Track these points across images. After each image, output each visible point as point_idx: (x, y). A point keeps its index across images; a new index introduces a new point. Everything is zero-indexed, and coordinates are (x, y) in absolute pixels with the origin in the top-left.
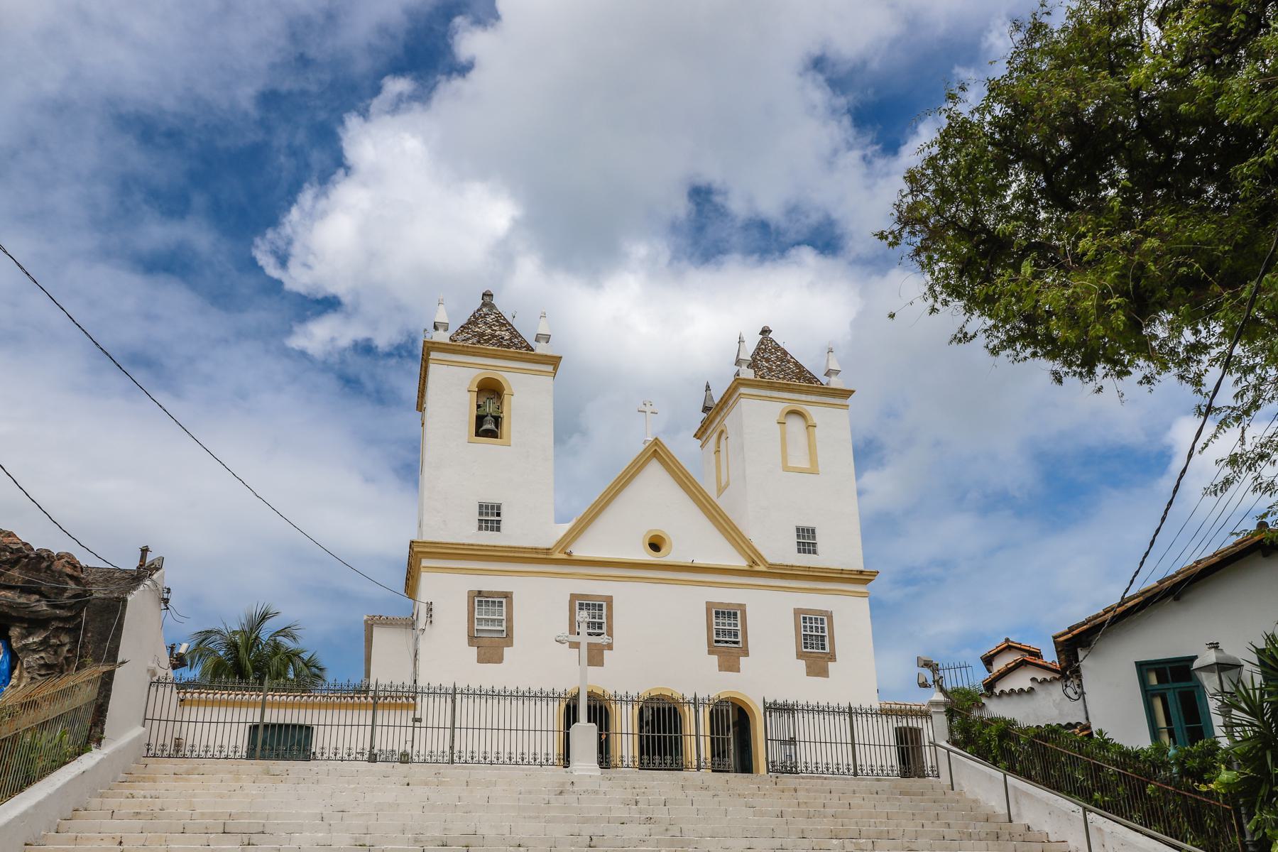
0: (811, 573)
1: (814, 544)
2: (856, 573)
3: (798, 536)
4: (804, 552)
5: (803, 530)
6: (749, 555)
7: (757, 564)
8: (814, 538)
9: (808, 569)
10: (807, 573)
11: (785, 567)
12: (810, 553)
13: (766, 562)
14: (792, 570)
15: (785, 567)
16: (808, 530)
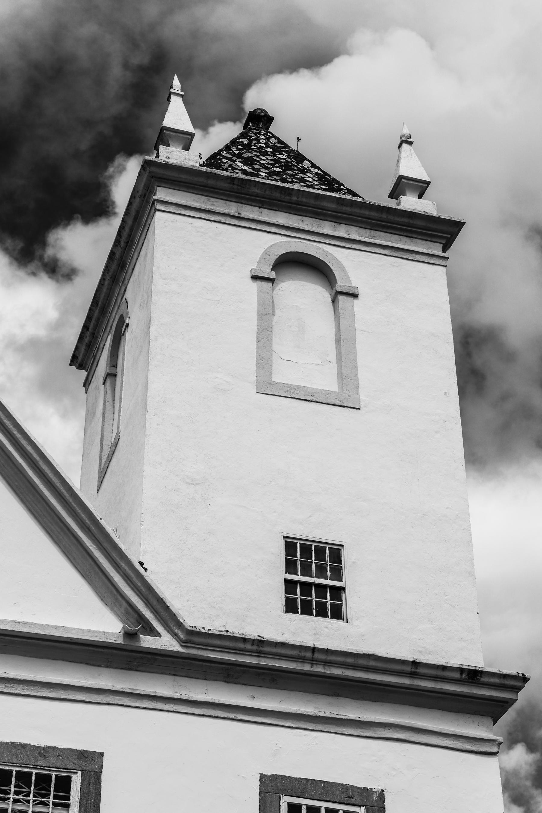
0: (319, 669)
1: (337, 592)
2: (457, 675)
3: (290, 566)
4: (307, 610)
5: (306, 549)
6: (131, 605)
7: (152, 631)
8: (337, 573)
9: (309, 655)
10: (307, 667)
11: (241, 645)
12: (322, 613)
13: (180, 625)
14: (259, 654)
15: (241, 645)
16: (320, 552)
